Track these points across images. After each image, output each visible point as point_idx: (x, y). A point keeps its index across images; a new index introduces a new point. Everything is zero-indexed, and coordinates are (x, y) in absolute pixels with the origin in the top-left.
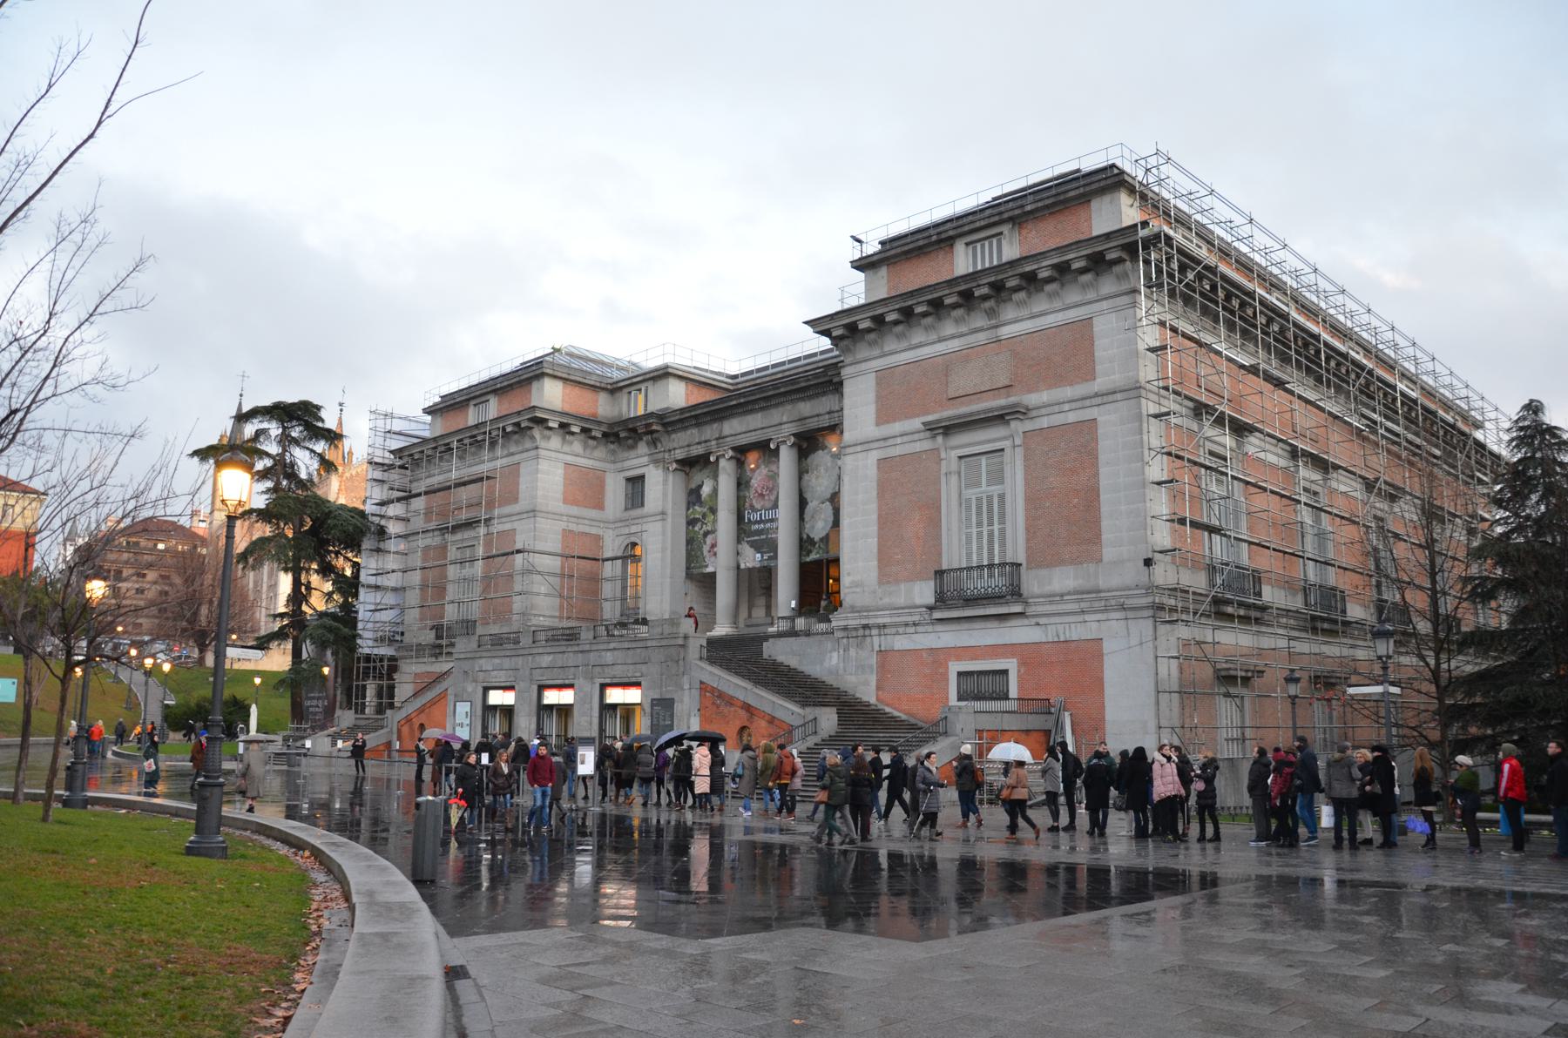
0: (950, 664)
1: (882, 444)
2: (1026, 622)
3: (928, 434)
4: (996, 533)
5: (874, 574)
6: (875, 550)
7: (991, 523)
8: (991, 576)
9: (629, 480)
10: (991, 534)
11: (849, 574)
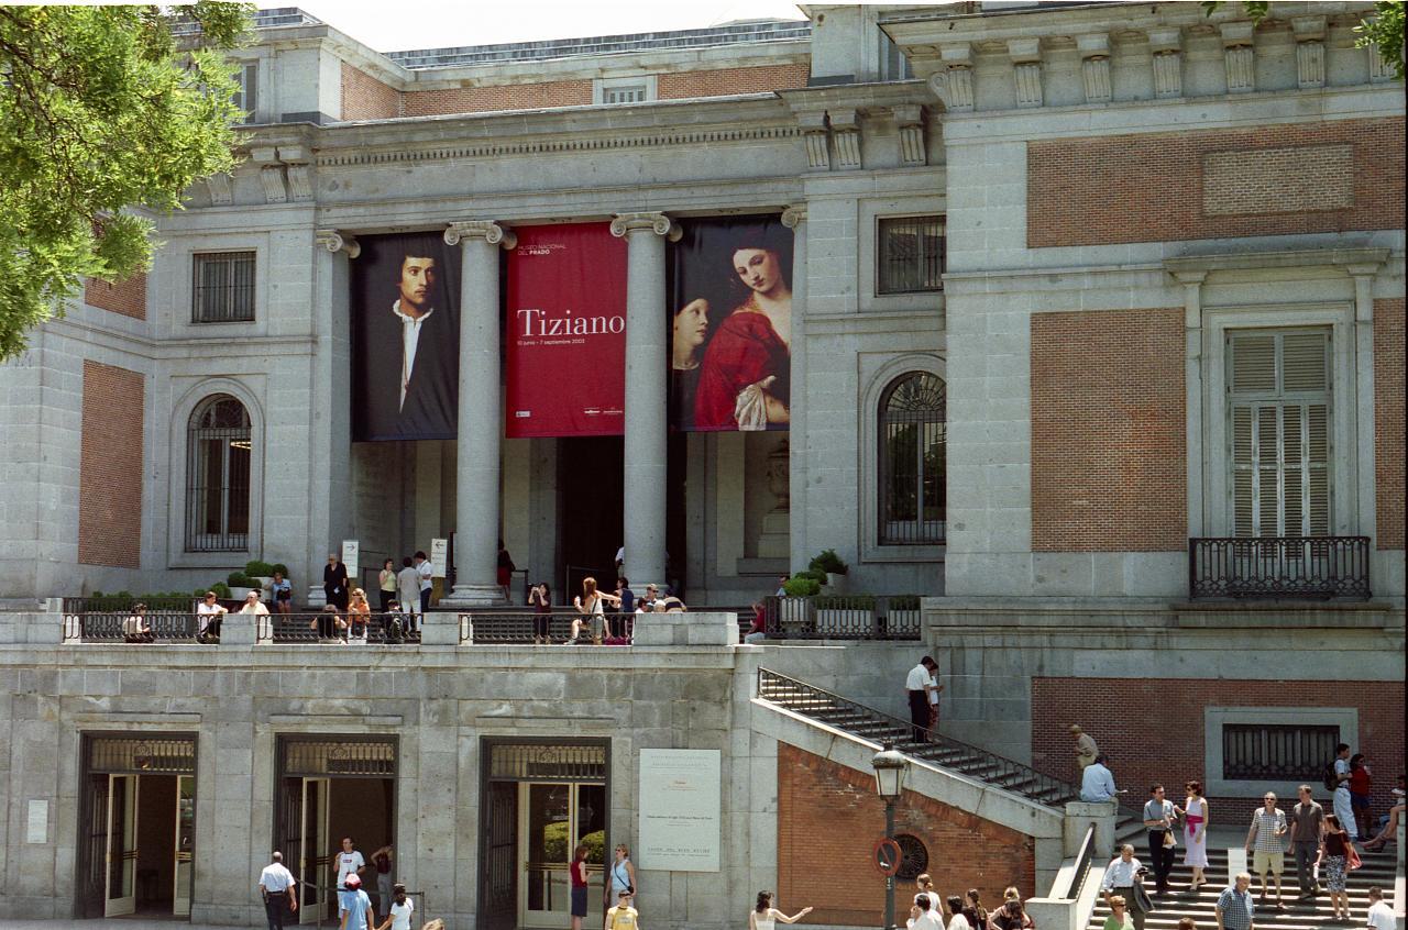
0: (1207, 711)
1: (1045, 284)
2: (1381, 643)
3: (1158, 279)
4: (1306, 478)
5: (1023, 532)
6: (1026, 485)
7: (1293, 456)
8: (1294, 553)
9: (197, 257)
11: (960, 527)
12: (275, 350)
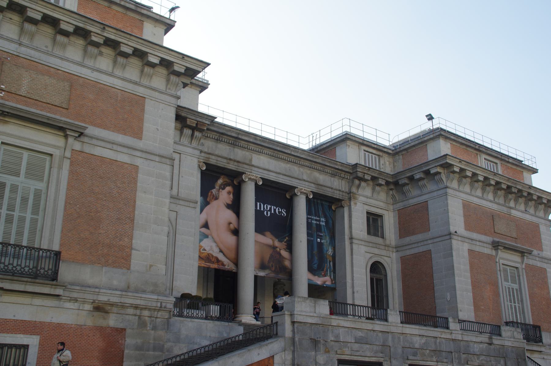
1: (470, 241)
3: (490, 246)
6: (472, 301)
7: (515, 303)
10: (515, 307)
11: (461, 311)
12: (181, 202)
